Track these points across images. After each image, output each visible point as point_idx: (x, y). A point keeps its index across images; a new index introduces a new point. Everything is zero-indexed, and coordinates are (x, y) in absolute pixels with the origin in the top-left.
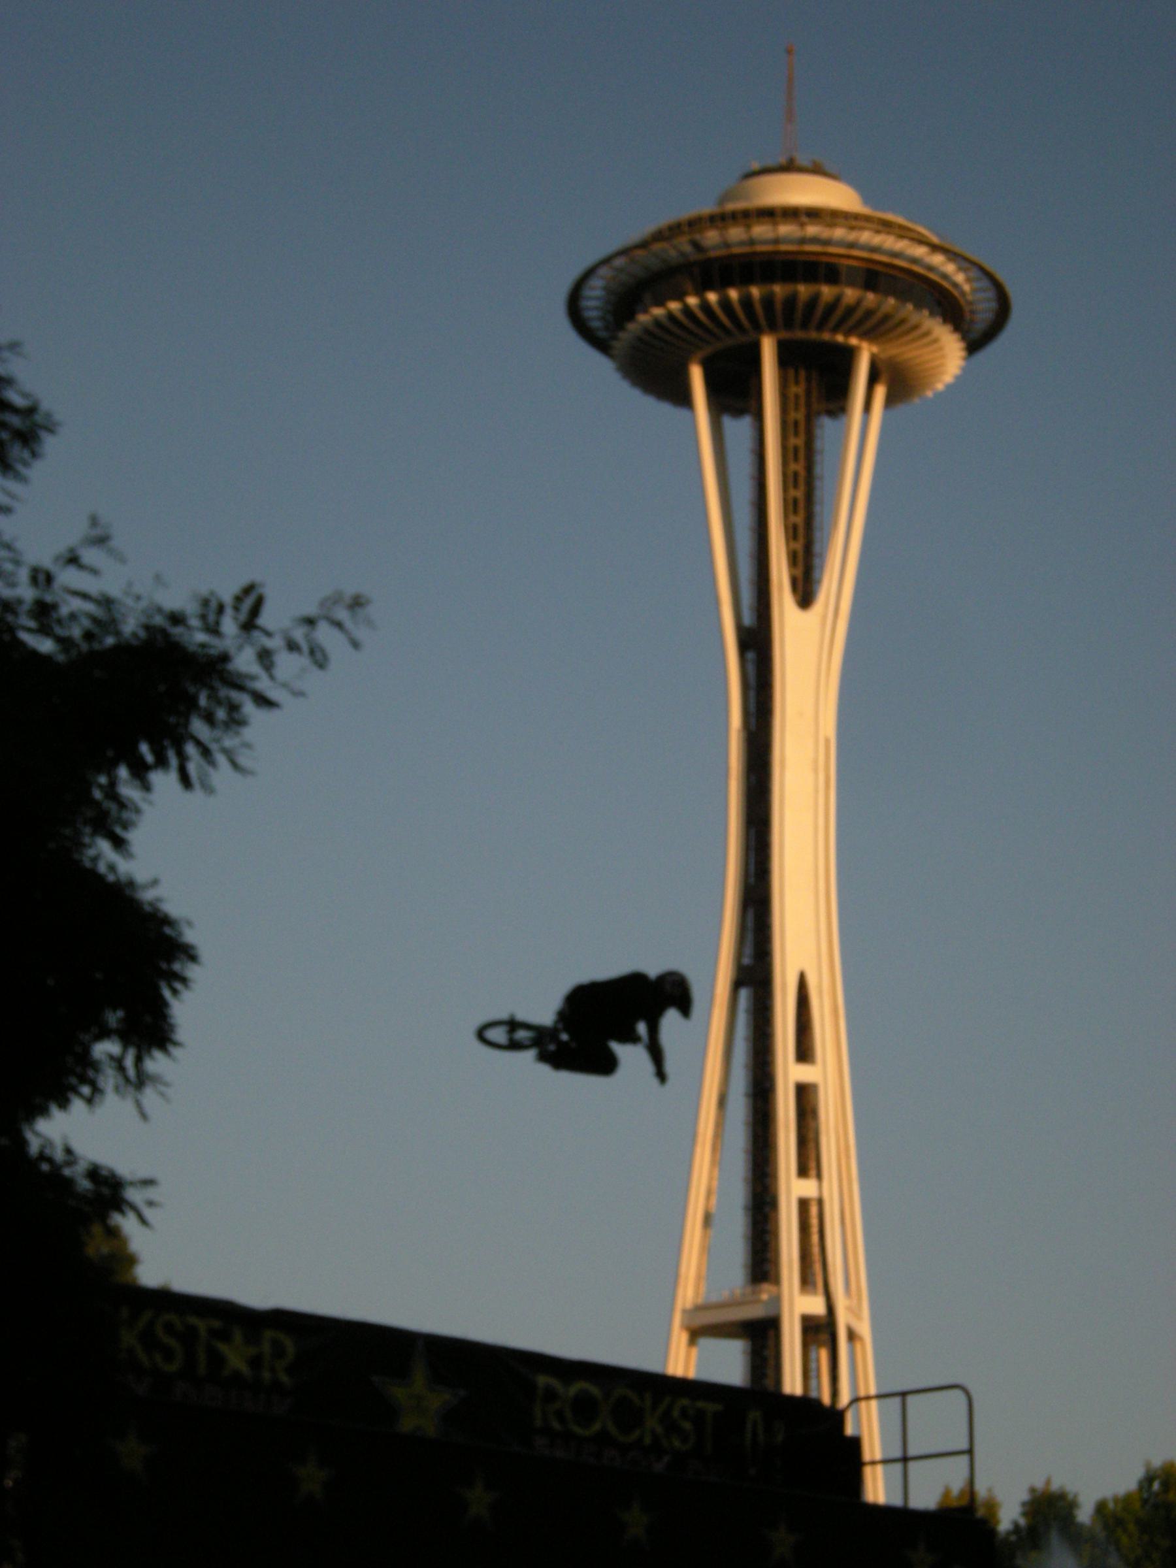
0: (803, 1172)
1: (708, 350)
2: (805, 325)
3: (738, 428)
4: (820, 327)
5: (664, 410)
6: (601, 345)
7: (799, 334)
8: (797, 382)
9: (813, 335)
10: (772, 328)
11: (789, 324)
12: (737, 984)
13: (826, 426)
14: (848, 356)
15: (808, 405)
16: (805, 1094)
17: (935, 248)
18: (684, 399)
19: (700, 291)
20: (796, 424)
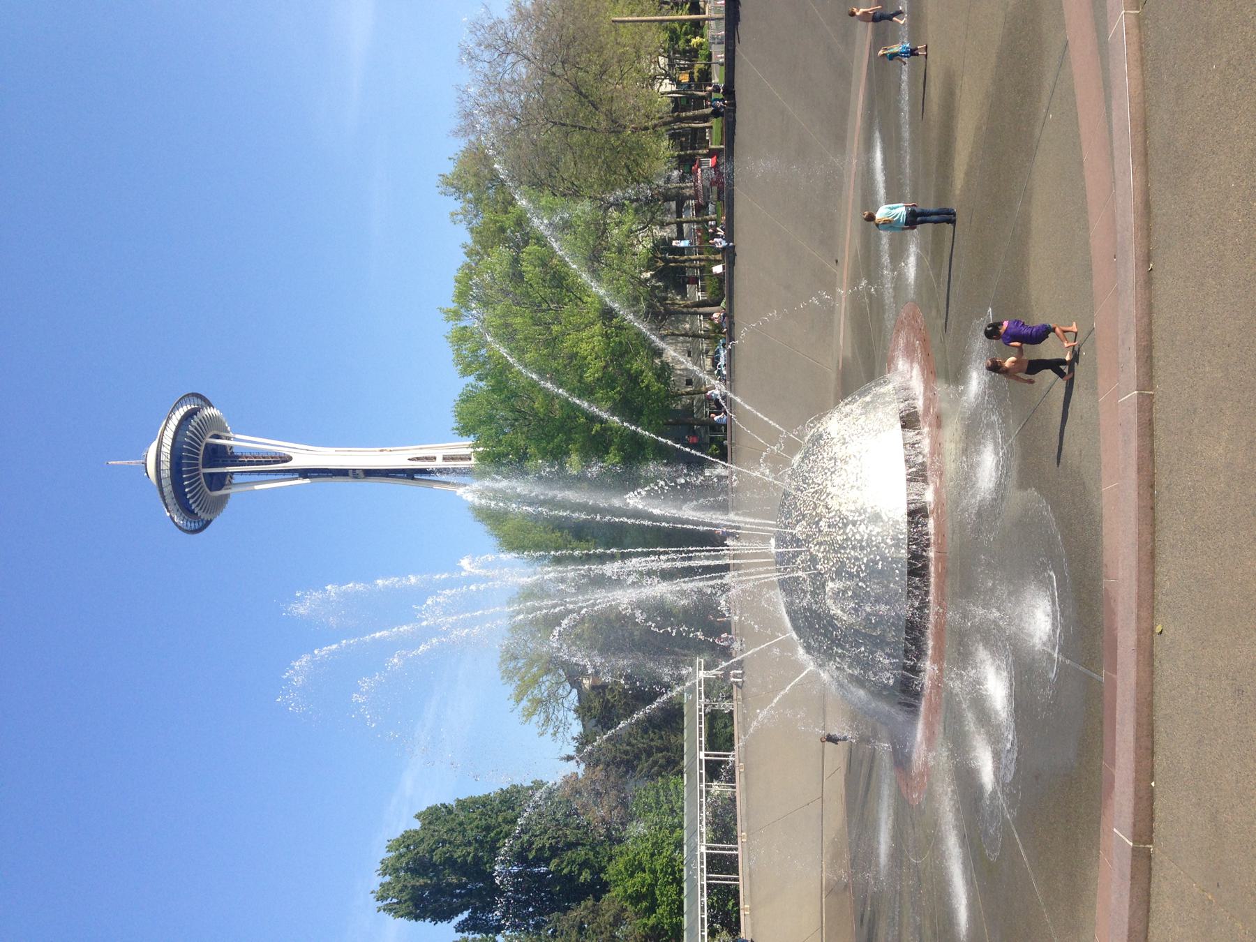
0: (470, 459)
1: (207, 490)
2: (197, 459)
3: (237, 479)
4: (198, 455)
5: (230, 502)
6: (209, 522)
7: (201, 461)
8: (218, 461)
9: (201, 457)
10: (198, 470)
11: (197, 465)
12: (413, 478)
13: (237, 452)
14: (207, 445)
15: (225, 457)
16: (445, 459)
17: (169, 418)
18: (227, 496)
19: (186, 494)
20: (232, 461)
